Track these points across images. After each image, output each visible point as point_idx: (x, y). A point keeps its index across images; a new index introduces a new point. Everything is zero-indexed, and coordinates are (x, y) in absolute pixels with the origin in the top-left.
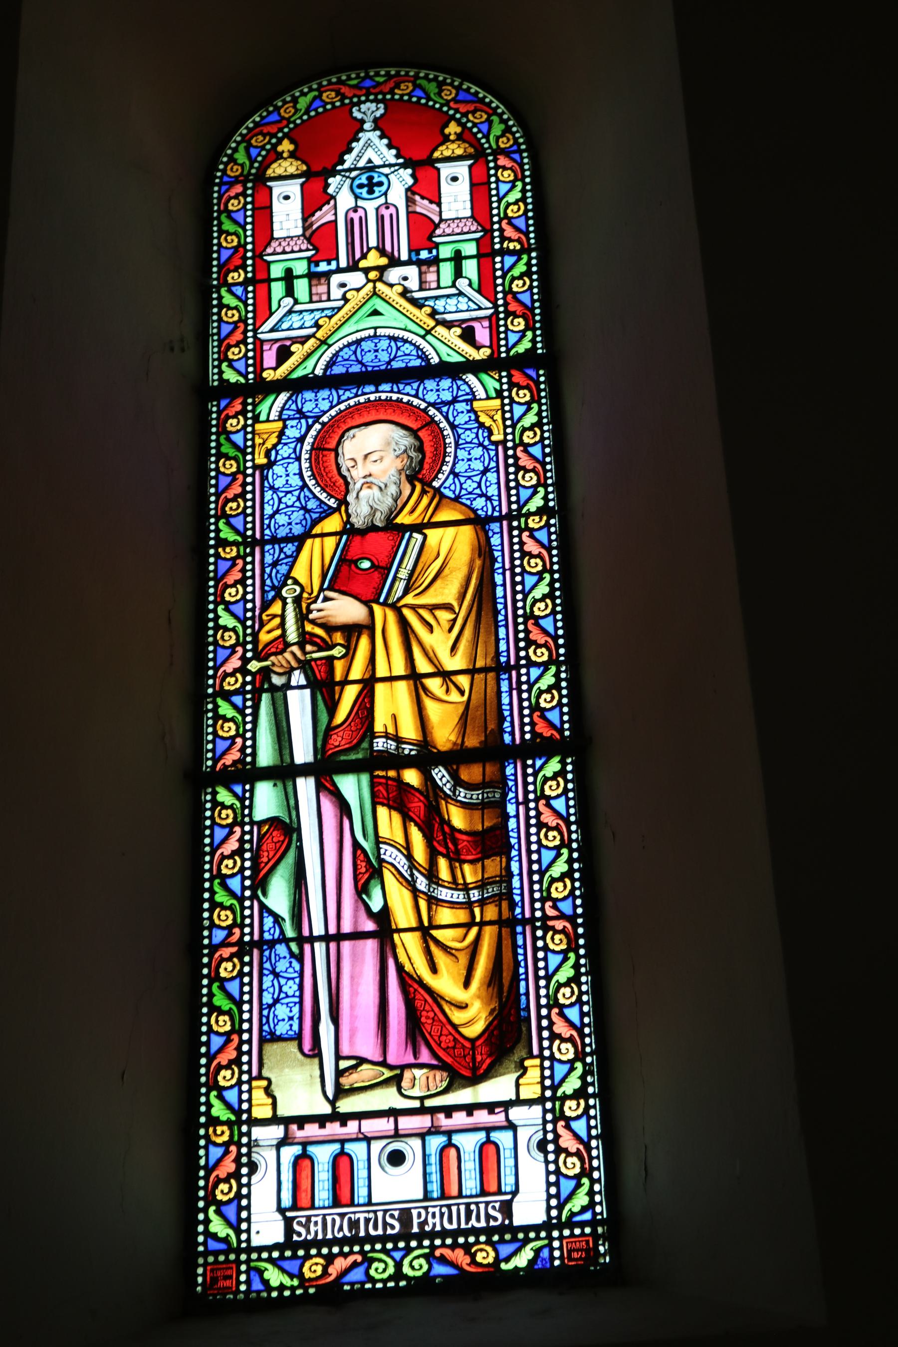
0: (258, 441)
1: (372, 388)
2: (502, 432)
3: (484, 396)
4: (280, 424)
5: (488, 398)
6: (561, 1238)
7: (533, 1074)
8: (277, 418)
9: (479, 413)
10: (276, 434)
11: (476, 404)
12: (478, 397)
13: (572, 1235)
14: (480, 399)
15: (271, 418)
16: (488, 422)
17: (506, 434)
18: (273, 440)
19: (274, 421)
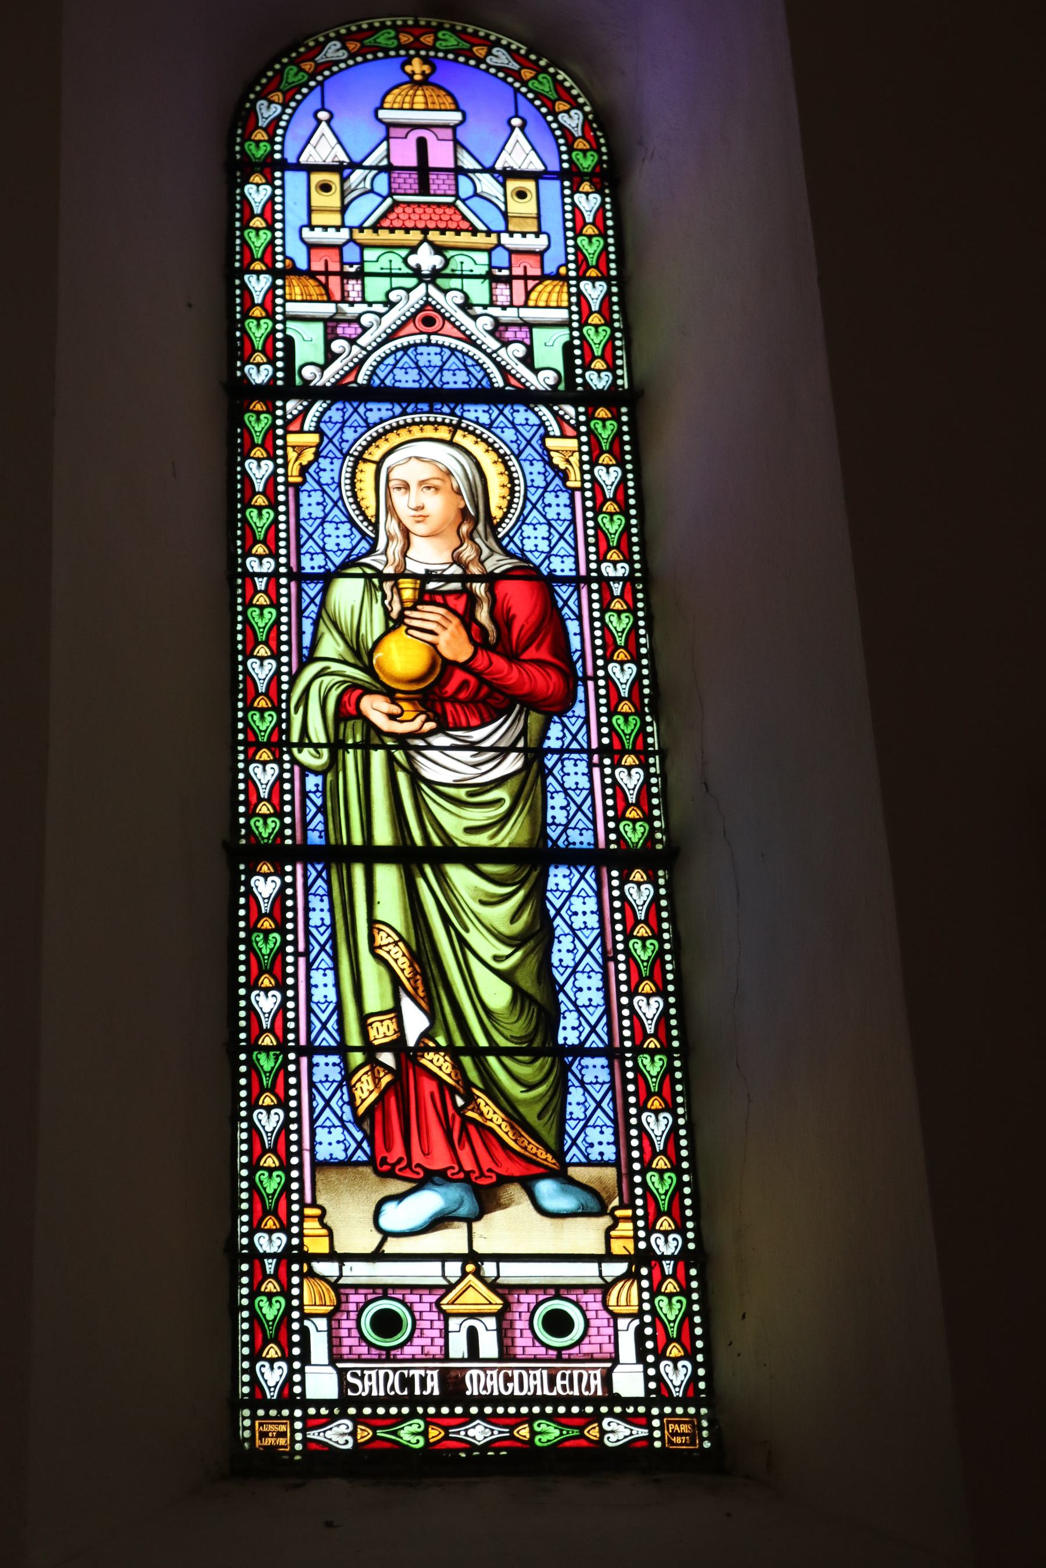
0: (292, 455)
1: (425, 407)
2: (579, 478)
3: (558, 433)
4: (315, 438)
5: (563, 436)
6: (661, 1416)
7: (625, 1228)
8: (312, 429)
9: (552, 454)
10: (313, 450)
11: (550, 443)
12: (552, 434)
13: (673, 1414)
14: (554, 437)
15: (306, 428)
16: (563, 465)
17: (583, 481)
18: (308, 455)
19: (309, 432)
